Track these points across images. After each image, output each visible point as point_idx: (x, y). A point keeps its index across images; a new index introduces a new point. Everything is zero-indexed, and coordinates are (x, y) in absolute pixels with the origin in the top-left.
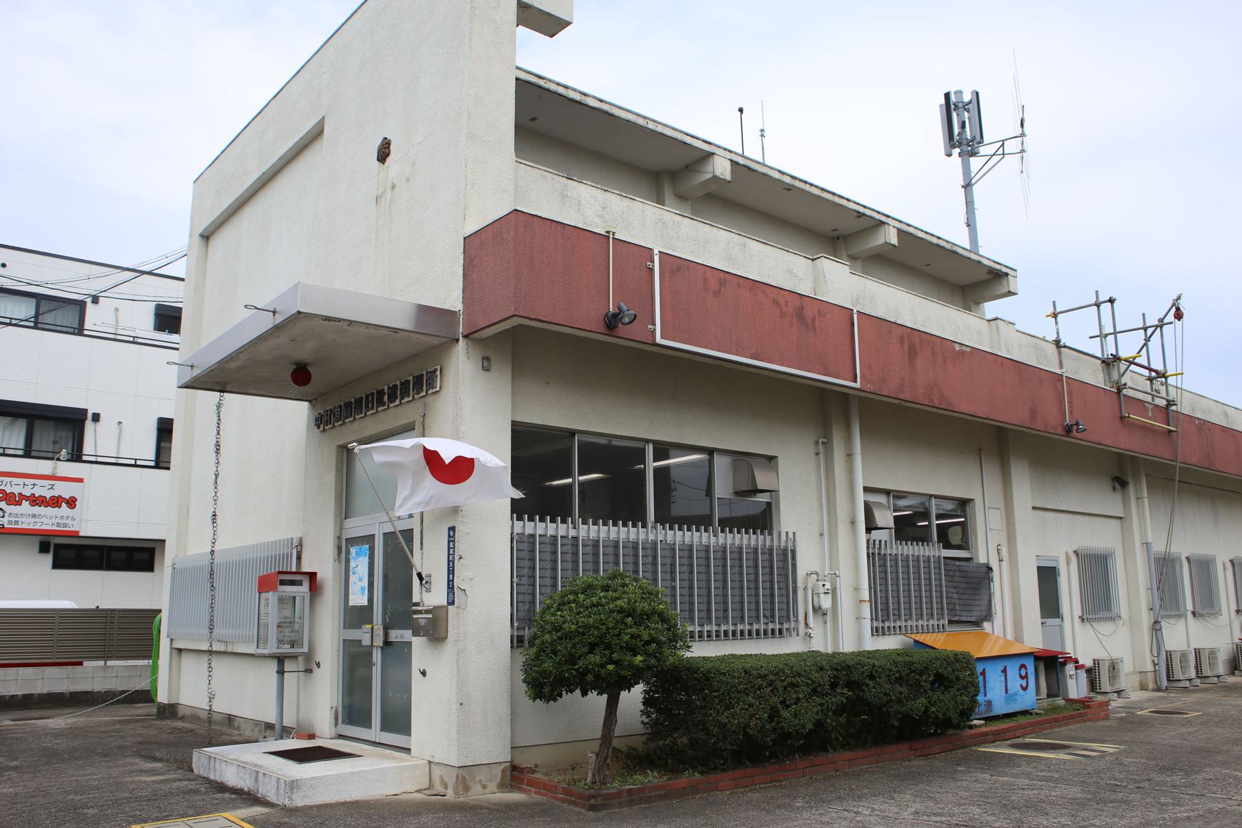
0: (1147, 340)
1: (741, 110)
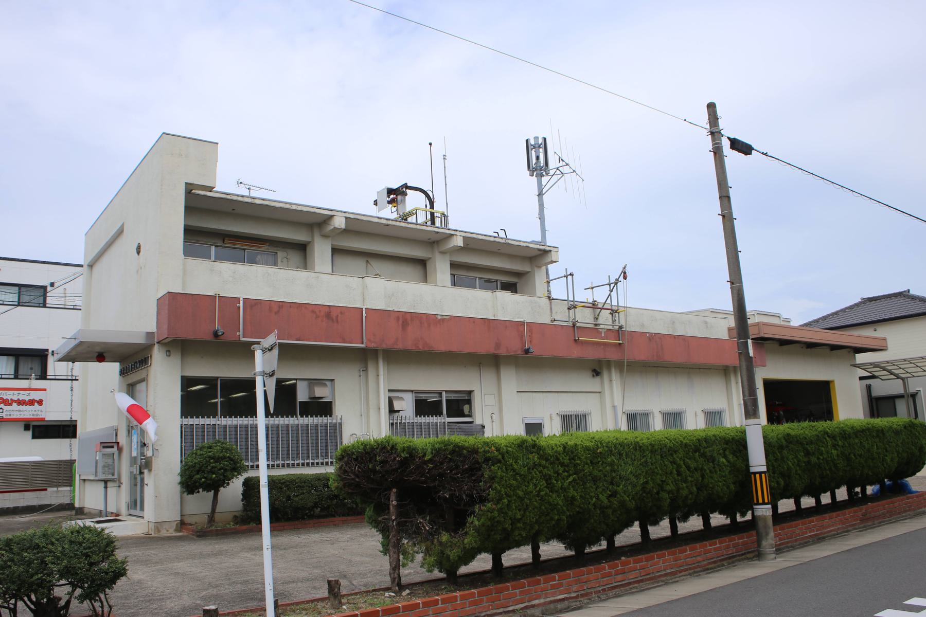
0: (611, 291)
1: (430, 144)
